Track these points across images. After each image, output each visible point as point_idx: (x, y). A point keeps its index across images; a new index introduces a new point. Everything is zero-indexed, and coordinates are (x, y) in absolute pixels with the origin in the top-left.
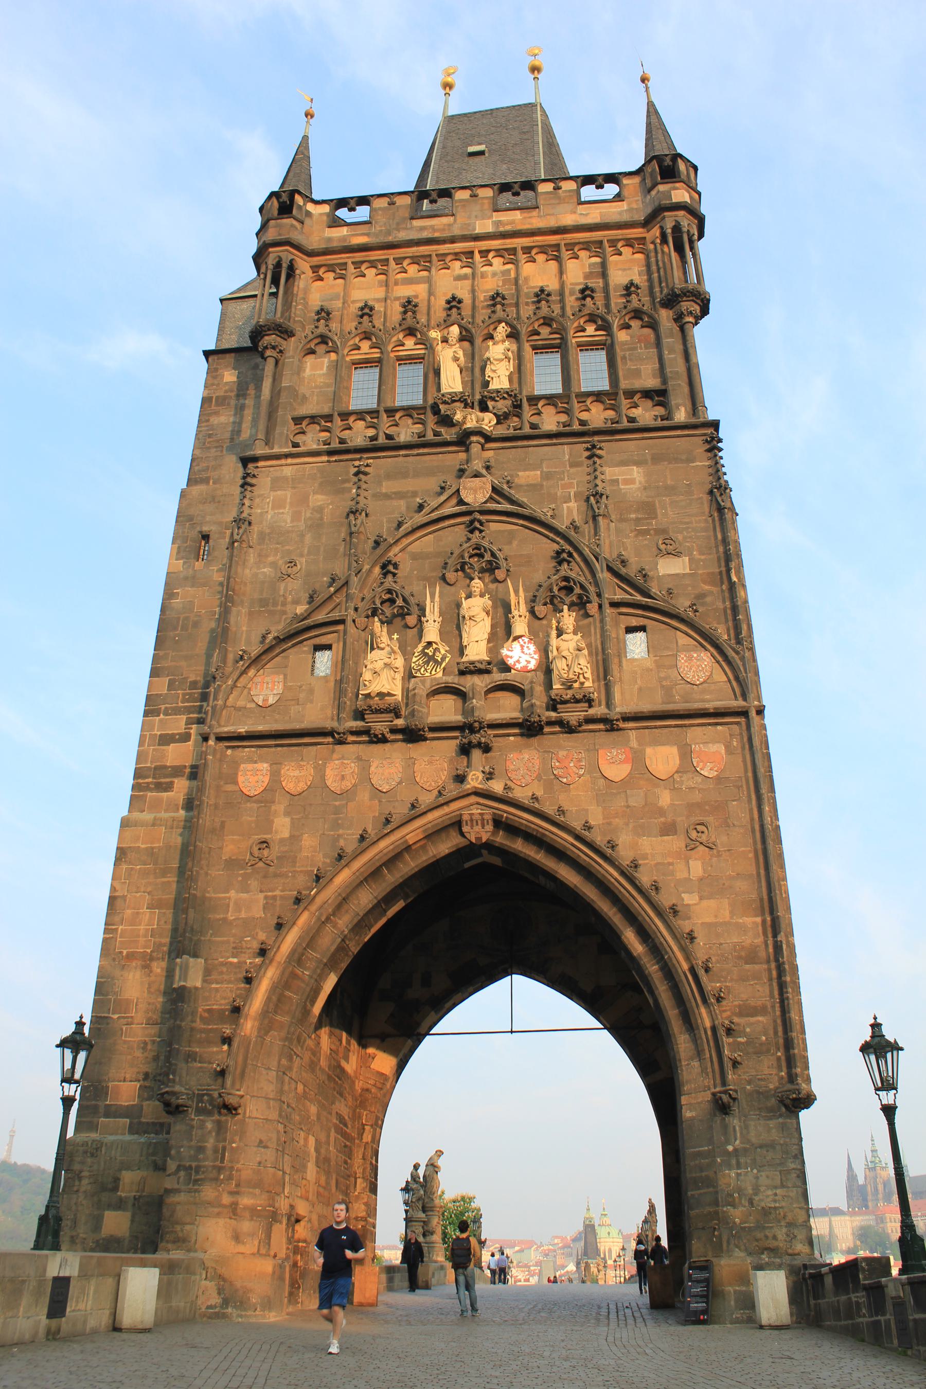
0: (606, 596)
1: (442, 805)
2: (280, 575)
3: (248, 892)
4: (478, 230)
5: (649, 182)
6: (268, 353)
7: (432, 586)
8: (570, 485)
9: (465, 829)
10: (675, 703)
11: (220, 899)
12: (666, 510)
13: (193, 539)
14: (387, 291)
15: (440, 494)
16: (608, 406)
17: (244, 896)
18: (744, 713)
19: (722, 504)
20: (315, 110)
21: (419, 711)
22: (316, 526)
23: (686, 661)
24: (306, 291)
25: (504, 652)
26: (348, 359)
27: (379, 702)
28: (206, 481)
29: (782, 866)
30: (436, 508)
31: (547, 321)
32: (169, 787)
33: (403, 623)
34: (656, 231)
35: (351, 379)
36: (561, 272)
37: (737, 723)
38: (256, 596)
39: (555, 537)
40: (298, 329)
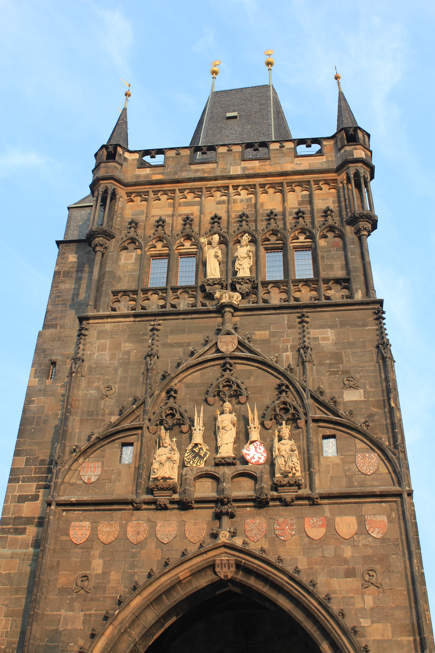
0: (310, 415)
1: (203, 553)
2: (101, 395)
3: (72, 610)
4: (232, 172)
5: (339, 144)
6: (98, 248)
7: (199, 406)
8: (288, 341)
9: (217, 570)
10: (354, 487)
11: (54, 615)
12: (349, 358)
13: (45, 365)
14: (174, 210)
15: (205, 345)
16: (312, 289)
17: (70, 613)
18: (400, 495)
19: (385, 355)
20: (131, 92)
21: (189, 490)
22: (125, 363)
23: (361, 459)
24: (123, 209)
25: (244, 451)
26: (148, 253)
27: (163, 483)
28: (55, 326)
29: (426, 601)
30: (202, 355)
31: (275, 233)
32: (23, 532)
33: (179, 430)
34: (343, 176)
35: (150, 267)
36: (284, 200)
37: (395, 502)
38: (85, 409)
39: (278, 375)
40: (116, 232)
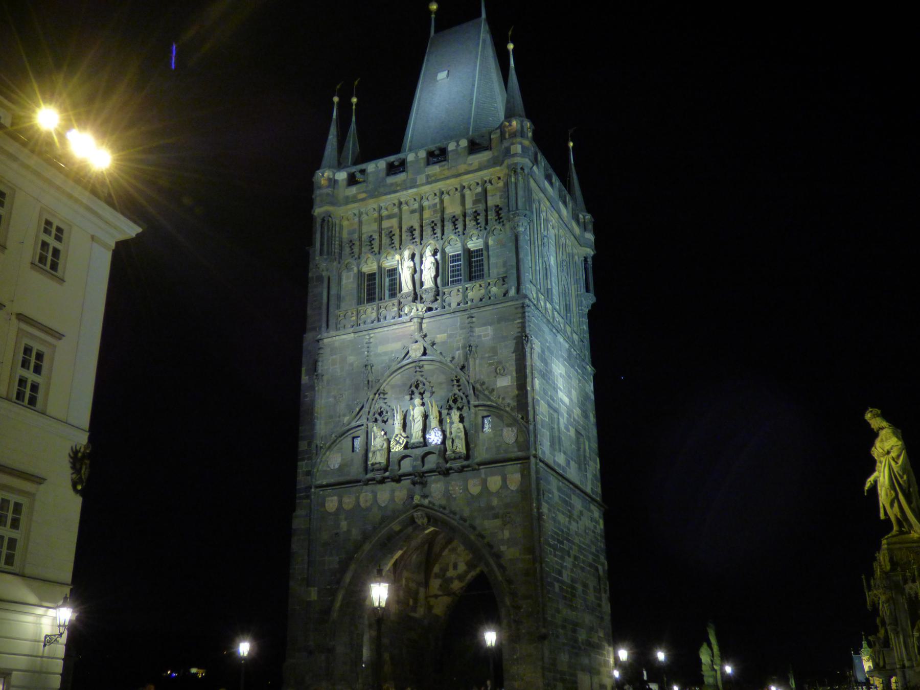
25: (428, 436)
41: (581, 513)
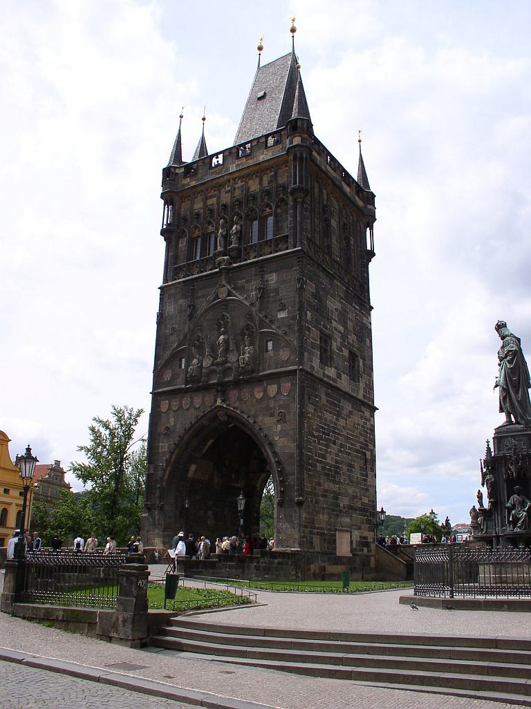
9: (220, 418)
18: (295, 371)
22: (180, 312)
24: (180, 208)
41: (351, 413)
